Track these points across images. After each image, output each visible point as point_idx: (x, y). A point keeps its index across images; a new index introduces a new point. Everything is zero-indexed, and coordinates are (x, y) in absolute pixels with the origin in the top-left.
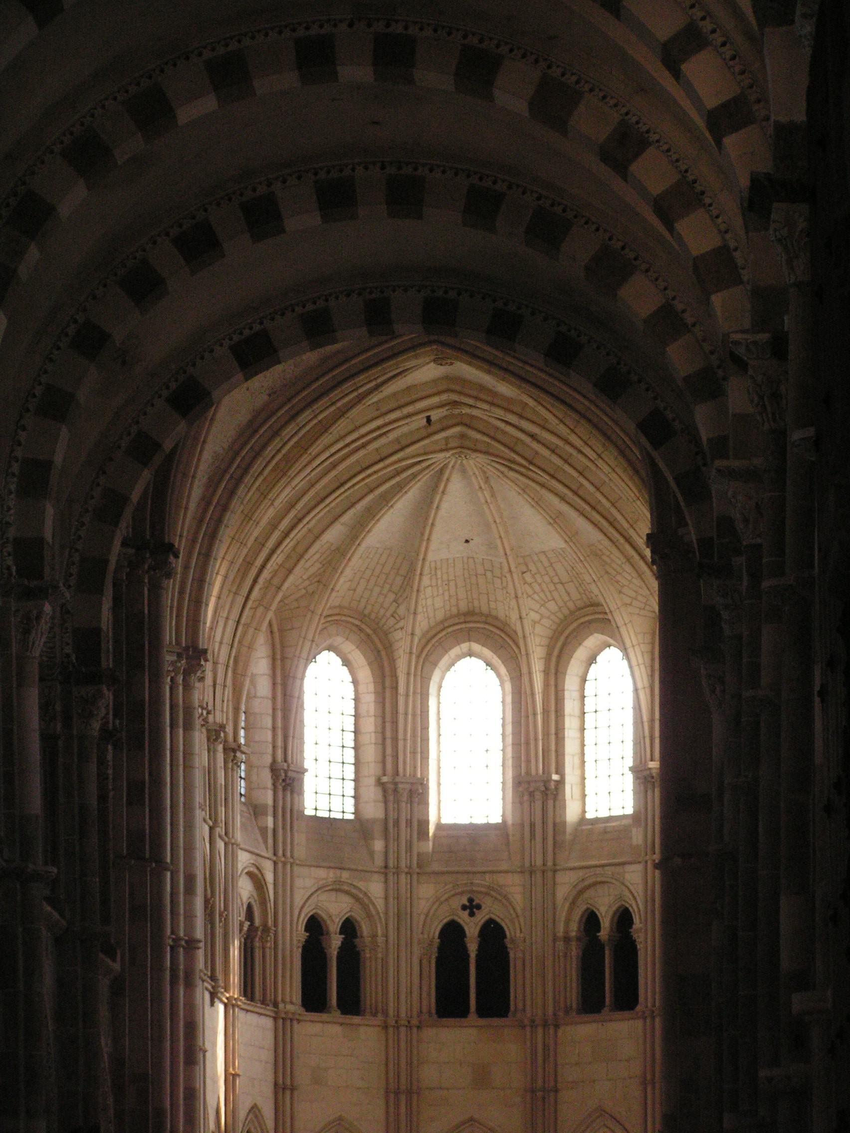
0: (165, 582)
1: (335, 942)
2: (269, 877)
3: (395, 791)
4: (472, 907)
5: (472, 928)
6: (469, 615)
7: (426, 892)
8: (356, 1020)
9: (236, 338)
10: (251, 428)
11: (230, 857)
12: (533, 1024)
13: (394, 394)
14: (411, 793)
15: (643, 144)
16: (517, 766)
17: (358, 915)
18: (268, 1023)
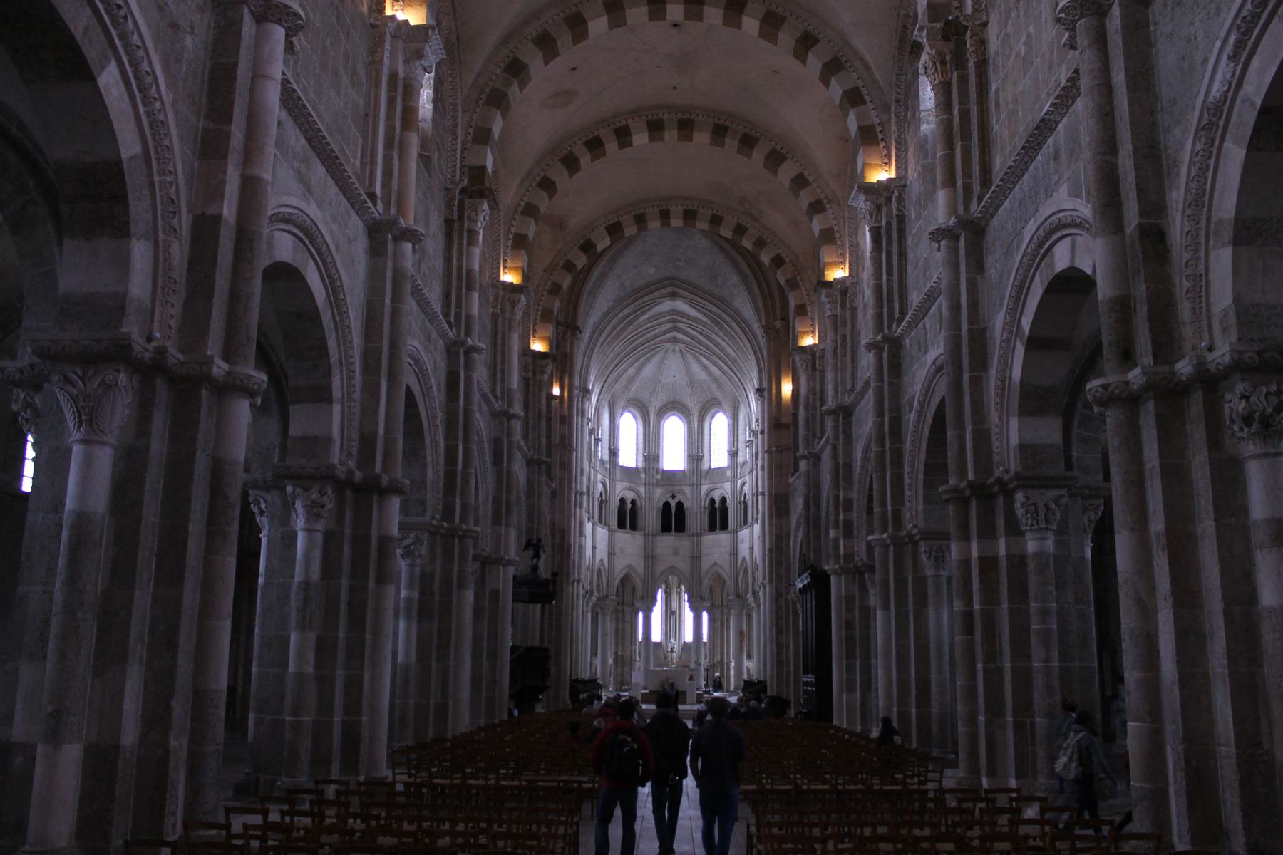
0: (576, 342)
1: (629, 506)
2: (608, 484)
3: (649, 458)
4: (673, 497)
5: (673, 504)
6: (673, 402)
7: (659, 491)
8: (635, 532)
9: (608, 223)
10: (607, 313)
11: (595, 475)
12: (693, 535)
13: (654, 316)
14: (654, 459)
15: (816, 41)
16: (688, 451)
17: (637, 499)
18: (607, 532)
